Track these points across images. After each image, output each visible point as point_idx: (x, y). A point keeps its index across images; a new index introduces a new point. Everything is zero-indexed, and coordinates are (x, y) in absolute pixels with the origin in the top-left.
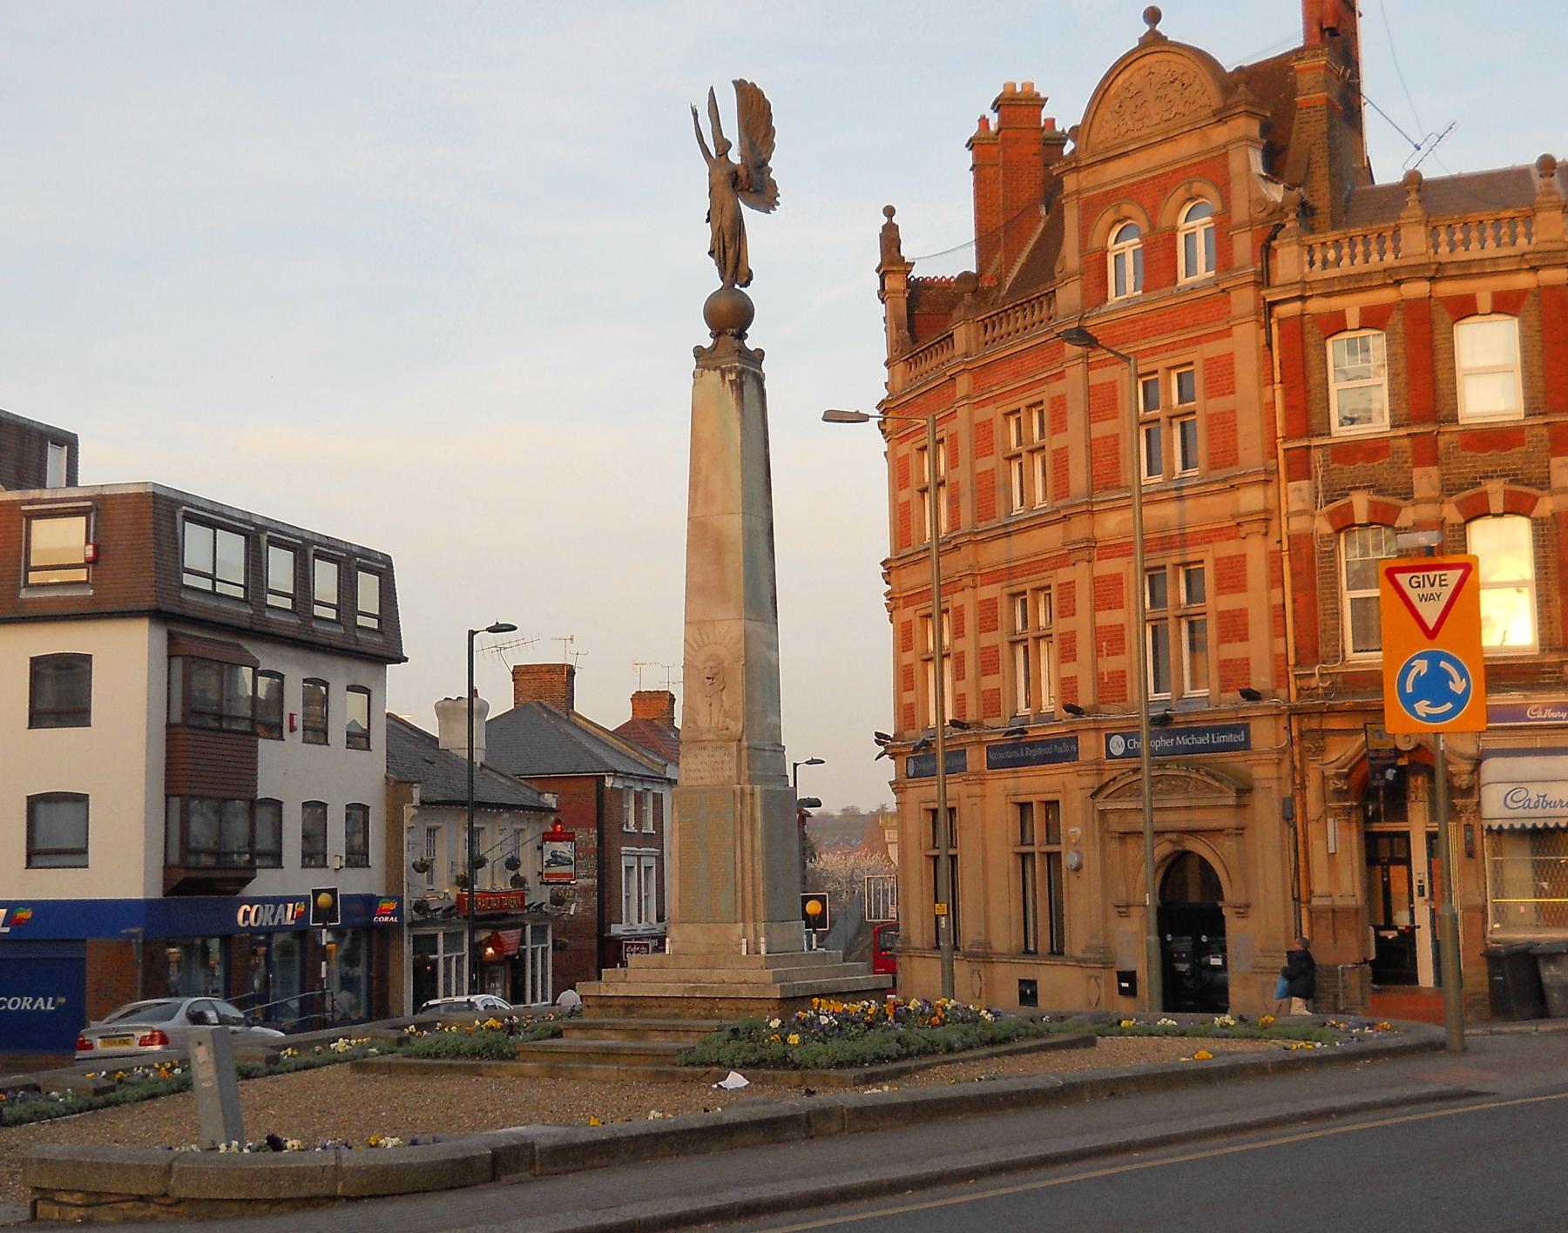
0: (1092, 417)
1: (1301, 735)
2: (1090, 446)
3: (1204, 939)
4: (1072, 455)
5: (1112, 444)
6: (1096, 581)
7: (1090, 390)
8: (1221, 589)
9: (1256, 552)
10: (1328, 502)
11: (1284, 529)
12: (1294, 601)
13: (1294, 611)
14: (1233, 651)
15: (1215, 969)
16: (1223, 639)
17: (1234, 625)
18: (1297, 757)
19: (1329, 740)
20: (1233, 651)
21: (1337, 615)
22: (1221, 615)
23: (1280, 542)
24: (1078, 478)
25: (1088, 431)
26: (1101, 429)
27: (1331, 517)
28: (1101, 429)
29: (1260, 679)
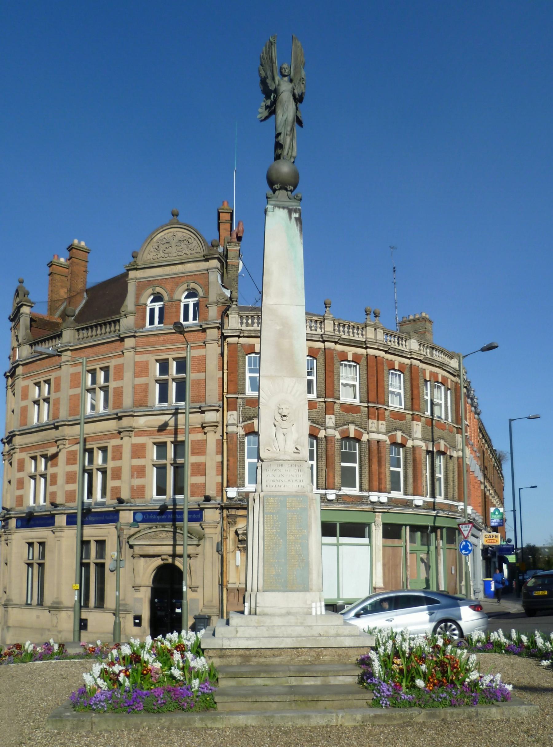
0: (136, 375)
1: (227, 516)
2: (134, 388)
3: (174, 601)
4: (125, 390)
5: (145, 389)
6: (133, 446)
7: (136, 364)
8: (193, 454)
9: (212, 439)
10: (244, 421)
11: (225, 431)
12: (228, 461)
13: (228, 465)
14: (199, 480)
15: (178, 613)
16: (193, 474)
17: (200, 469)
18: (225, 526)
19: (238, 519)
20: (199, 480)
21: (243, 468)
22: (193, 464)
23: (222, 436)
24: (127, 401)
25: (134, 381)
26: (139, 381)
27: (244, 427)
28: (139, 381)
29: (211, 491)
